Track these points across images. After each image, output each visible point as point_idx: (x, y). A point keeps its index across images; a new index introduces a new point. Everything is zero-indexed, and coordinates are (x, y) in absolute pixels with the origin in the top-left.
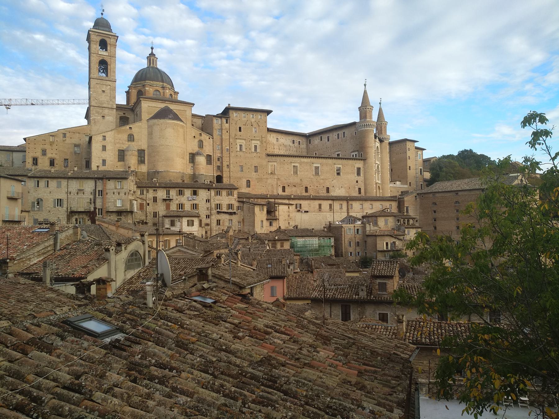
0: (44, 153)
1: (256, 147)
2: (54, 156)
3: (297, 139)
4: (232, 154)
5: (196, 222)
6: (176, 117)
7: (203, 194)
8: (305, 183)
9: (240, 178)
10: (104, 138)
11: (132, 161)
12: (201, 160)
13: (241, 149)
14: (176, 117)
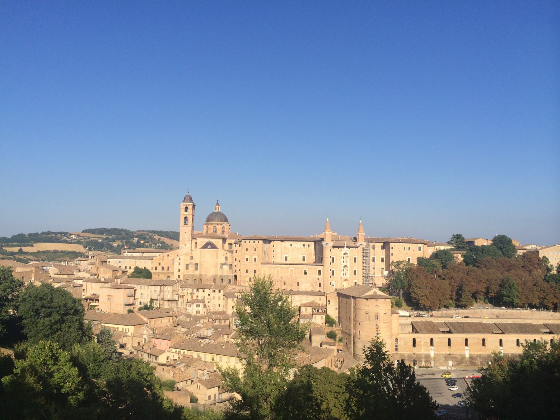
0: (160, 264)
1: (255, 259)
2: (163, 266)
3: (307, 243)
4: (243, 264)
5: (201, 305)
6: (213, 246)
7: (207, 291)
8: (284, 280)
9: (246, 277)
10: (180, 259)
11: (191, 268)
12: (226, 268)
13: (247, 260)
14: (213, 246)
